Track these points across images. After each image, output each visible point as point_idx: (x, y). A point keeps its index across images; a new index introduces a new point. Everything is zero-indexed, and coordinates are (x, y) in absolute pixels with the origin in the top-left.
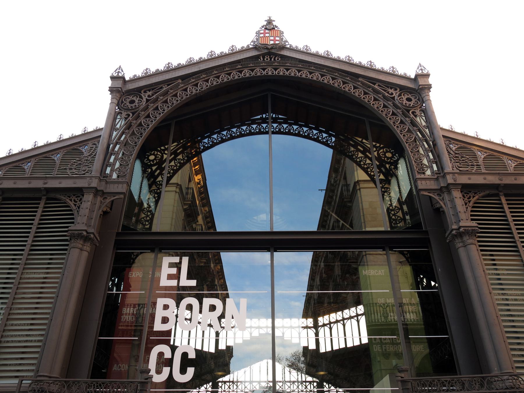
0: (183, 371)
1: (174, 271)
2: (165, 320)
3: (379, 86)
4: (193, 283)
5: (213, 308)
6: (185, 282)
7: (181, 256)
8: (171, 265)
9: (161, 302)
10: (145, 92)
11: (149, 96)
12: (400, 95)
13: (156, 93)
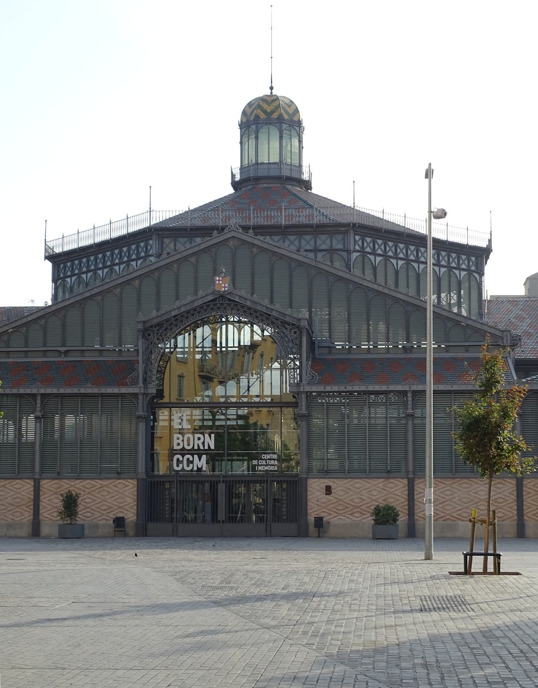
0: (188, 466)
3: (281, 322)
9: (176, 436)
10: (155, 327)
11: (158, 331)
12: (291, 329)
13: (161, 328)
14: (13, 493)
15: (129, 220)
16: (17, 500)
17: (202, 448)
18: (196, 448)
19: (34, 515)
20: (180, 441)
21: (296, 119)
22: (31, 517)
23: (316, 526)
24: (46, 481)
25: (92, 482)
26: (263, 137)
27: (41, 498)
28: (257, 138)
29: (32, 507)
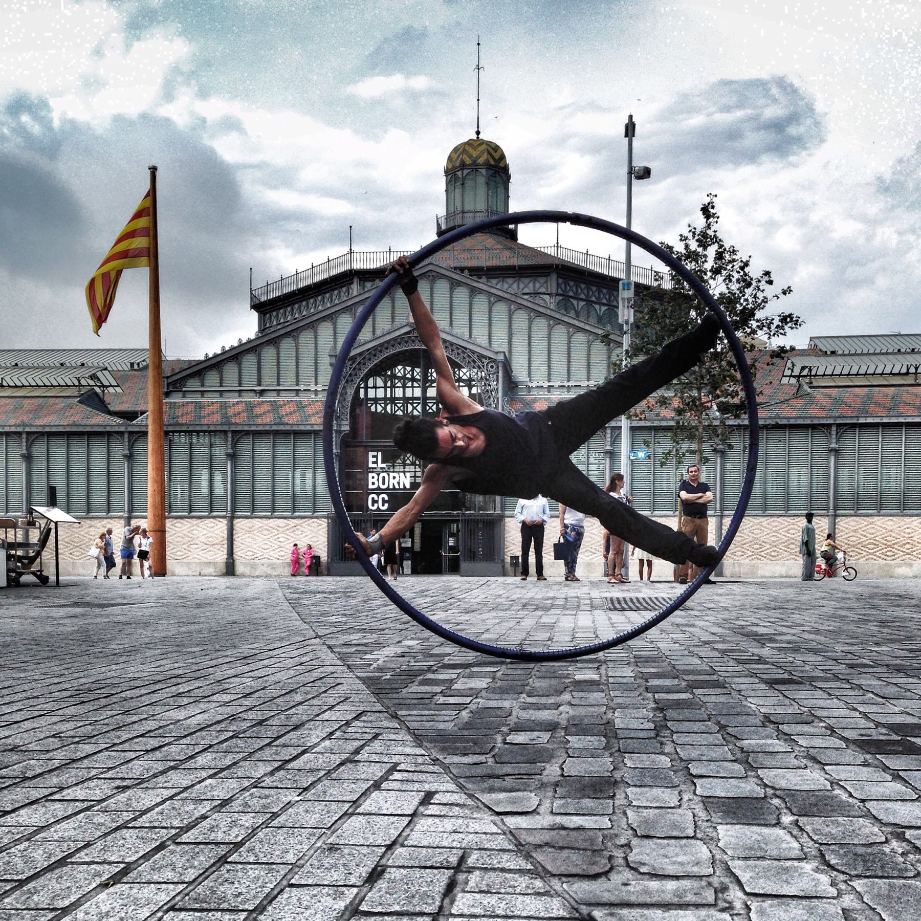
1: (375, 459)
2: (373, 484)
4: (384, 465)
5: (394, 478)
6: (380, 465)
7: (378, 451)
8: (373, 457)
9: (370, 475)
14: (206, 532)
15: (331, 263)
16: (211, 539)
17: (397, 487)
18: (391, 487)
19: (228, 554)
20: (375, 480)
21: (502, 165)
22: (226, 556)
23: (512, 564)
24: (239, 520)
25: (285, 521)
26: (469, 184)
27: (235, 537)
28: (463, 184)
29: (226, 546)
